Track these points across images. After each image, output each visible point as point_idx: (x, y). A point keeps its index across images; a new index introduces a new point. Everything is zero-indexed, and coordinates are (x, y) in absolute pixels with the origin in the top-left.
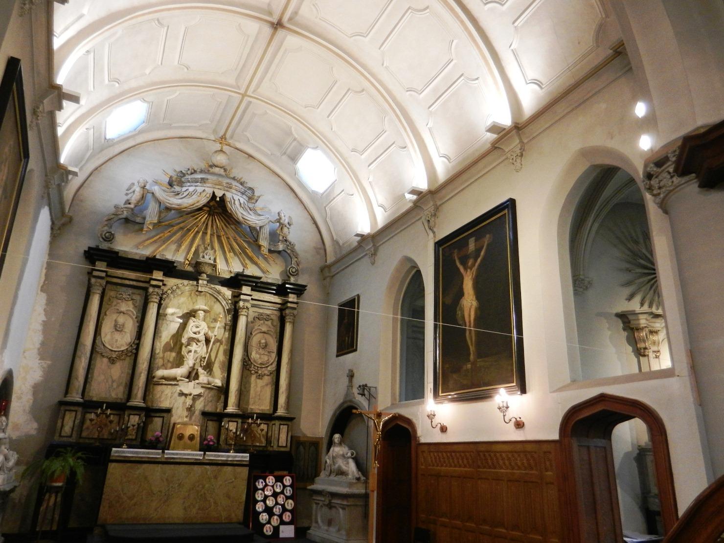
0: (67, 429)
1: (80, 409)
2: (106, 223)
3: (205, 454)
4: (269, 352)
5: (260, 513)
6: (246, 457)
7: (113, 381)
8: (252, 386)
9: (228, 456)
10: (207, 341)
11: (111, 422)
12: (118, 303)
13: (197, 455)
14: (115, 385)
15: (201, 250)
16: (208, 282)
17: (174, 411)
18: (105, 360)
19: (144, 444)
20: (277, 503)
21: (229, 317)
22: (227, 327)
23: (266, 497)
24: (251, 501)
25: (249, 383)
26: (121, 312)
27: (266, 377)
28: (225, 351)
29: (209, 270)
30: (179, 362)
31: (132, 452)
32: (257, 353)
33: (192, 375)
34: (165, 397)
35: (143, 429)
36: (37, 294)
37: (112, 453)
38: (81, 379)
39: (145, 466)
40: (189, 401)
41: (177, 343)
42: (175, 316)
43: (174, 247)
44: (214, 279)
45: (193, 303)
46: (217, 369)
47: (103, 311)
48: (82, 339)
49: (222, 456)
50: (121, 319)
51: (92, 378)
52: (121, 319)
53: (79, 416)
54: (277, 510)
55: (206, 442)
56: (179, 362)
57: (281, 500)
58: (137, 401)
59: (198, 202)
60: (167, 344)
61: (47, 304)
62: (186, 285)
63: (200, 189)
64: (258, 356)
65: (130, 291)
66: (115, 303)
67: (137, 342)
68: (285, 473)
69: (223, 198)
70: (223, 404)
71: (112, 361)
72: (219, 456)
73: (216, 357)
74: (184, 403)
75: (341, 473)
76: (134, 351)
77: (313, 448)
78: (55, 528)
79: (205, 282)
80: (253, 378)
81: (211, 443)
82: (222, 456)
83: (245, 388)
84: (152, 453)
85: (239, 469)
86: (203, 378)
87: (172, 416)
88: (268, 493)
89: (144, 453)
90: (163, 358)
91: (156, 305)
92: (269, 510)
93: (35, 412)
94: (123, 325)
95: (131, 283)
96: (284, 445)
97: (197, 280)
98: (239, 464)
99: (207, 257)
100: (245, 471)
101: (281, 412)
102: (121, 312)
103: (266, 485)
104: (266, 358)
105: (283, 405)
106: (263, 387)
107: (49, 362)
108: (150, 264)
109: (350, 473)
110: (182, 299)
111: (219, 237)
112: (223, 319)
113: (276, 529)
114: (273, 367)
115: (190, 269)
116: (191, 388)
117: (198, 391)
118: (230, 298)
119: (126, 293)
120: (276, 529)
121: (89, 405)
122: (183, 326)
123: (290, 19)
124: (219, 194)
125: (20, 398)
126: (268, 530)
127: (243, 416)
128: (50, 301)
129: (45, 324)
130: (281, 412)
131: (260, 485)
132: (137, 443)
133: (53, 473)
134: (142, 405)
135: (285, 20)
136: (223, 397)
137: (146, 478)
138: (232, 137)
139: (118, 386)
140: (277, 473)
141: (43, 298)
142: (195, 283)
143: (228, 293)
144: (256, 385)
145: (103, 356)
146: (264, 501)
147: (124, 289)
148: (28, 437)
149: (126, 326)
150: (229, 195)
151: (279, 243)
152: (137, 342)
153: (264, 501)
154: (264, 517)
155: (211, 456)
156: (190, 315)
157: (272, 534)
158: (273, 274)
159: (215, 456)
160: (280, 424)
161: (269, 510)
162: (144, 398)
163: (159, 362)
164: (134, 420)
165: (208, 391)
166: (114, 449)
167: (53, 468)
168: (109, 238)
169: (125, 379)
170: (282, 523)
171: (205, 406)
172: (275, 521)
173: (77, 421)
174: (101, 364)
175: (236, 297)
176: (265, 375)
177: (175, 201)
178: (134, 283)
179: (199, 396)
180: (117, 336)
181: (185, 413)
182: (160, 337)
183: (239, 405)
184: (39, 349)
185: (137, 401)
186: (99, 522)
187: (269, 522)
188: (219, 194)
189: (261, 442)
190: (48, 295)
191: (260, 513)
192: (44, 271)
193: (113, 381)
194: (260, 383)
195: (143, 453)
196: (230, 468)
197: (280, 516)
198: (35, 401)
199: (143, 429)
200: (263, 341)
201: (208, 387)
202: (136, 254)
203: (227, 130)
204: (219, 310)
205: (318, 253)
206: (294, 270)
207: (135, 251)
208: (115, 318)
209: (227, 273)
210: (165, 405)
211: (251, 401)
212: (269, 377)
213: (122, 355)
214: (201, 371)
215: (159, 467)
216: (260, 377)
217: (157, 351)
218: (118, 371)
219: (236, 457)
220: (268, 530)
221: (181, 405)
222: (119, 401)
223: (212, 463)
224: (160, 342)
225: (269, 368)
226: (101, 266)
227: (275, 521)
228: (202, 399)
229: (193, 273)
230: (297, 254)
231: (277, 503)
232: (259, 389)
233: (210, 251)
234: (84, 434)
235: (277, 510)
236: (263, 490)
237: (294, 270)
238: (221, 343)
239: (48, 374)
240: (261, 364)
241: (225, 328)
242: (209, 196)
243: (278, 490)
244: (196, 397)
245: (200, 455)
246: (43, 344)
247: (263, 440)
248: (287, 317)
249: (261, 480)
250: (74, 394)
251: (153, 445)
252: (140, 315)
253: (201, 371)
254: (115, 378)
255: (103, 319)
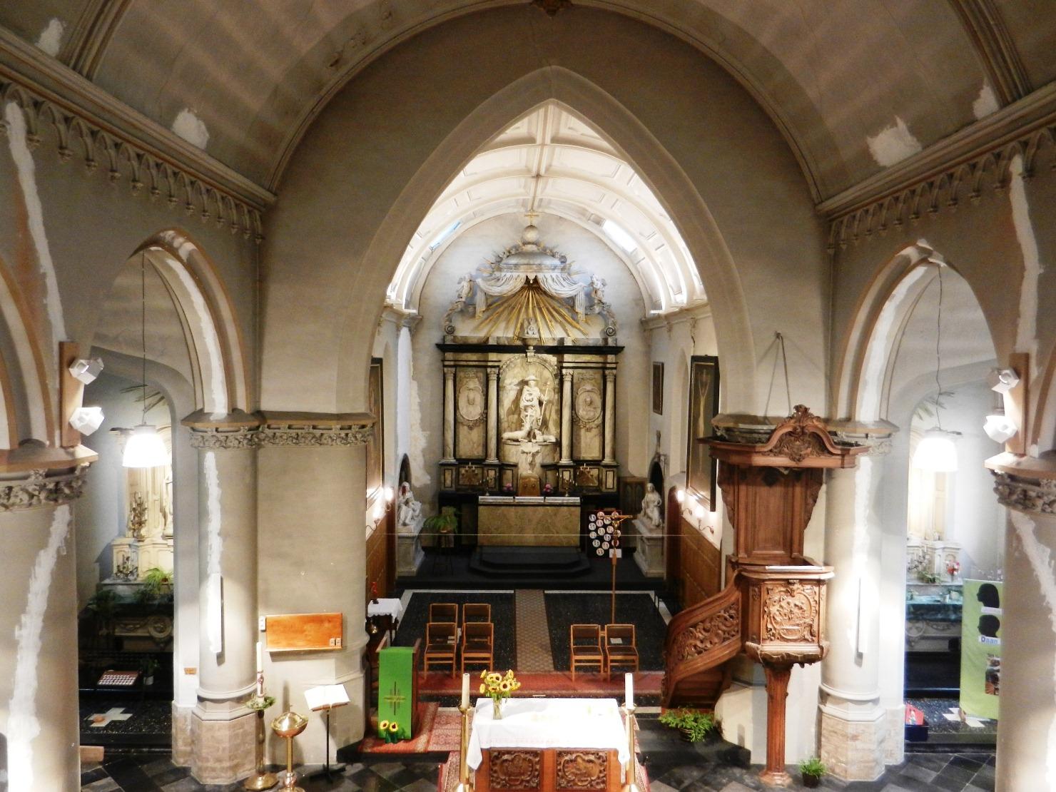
0: (448, 482)
1: (454, 468)
2: (446, 318)
3: (545, 498)
4: (595, 408)
5: (593, 540)
6: (577, 500)
7: (474, 443)
8: (582, 438)
9: (563, 500)
10: (541, 403)
11: (477, 474)
12: (467, 382)
13: (539, 499)
14: (475, 445)
15: (525, 326)
16: (535, 353)
17: (519, 466)
18: (466, 428)
19: (502, 493)
20: (606, 533)
21: (557, 381)
22: (556, 390)
23: (597, 528)
24: (585, 529)
25: (579, 435)
26: (470, 390)
27: (593, 429)
28: (557, 411)
29: (535, 343)
30: (520, 425)
31: (492, 499)
32: (584, 410)
33: (531, 436)
34: (512, 454)
35: (499, 479)
36: (410, 383)
37: (479, 500)
38: (451, 446)
39: (503, 508)
40: (530, 459)
41: (516, 407)
42: (512, 385)
43: (503, 325)
44: (541, 349)
45: (526, 371)
46: (551, 426)
47: (457, 389)
48: (446, 416)
49: (559, 500)
50: (472, 395)
51: (459, 441)
52: (472, 395)
53: (454, 473)
54: (607, 538)
55: (544, 490)
56: (520, 425)
57: (610, 529)
58: (492, 460)
59: (515, 288)
60: (510, 409)
61: (418, 390)
62: (517, 358)
63: (515, 275)
64: (585, 413)
65: (475, 370)
66: (465, 382)
67: (485, 411)
68: (613, 509)
69: (536, 280)
70: (559, 455)
71: (471, 428)
72: (556, 500)
73: (550, 415)
74: (526, 459)
75: (650, 518)
76: (485, 419)
77: (639, 487)
78: (452, 546)
79: (533, 354)
80: (583, 432)
81: (549, 491)
82: (559, 500)
83: (576, 440)
84: (506, 499)
85: (573, 509)
86: (540, 438)
87: (518, 469)
88: (600, 523)
89: (501, 499)
90: (508, 421)
91: (495, 382)
92: (601, 539)
93: (427, 467)
94: (474, 400)
95: (474, 363)
96: (611, 487)
97: (526, 353)
98: (574, 505)
99: (530, 333)
100: (578, 510)
101: (607, 460)
102: (470, 390)
103: (597, 519)
104: (592, 414)
105: (609, 455)
106: (592, 439)
107: (428, 432)
108: (483, 347)
109: (654, 519)
110: (516, 370)
111: (540, 309)
112: (552, 383)
113: (607, 552)
114: (600, 420)
115: (519, 343)
116: (531, 447)
117: (537, 448)
118: (556, 363)
119: (471, 372)
120: (607, 552)
121: (462, 462)
122: (520, 392)
123: (547, 170)
124: (532, 277)
125: (415, 460)
126: (600, 552)
127: (577, 463)
128: (420, 386)
129: (421, 405)
130: (607, 460)
131: (592, 518)
132: (496, 490)
133: (440, 527)
134: (496, 462)
135: (542, 172)
136: (558, 449)
137: (505, 516)
138: (539, 206)
139: (478, 446)
140: (605, 510)
141: (415, 384)
142: (524, 355)
143: (552, 359)
144: (586, 437)
145: (464, 425)
146: (596, 531)
147: (470, 369)
148: (426, 486)
149: (476, 400)
150: (540, 276)
151: (595, 307)
152: (485, 411)
153: (596, 531)
154: (596, 543)
155: (550, 500)
156: (524, 383)
157: (489, 603)
158: (593, 335)
159: (553, 500)
160: (606, 471)
161: (601, 539)
162: (498, 456)
163: (504, 425)
164: (492, 473)
165: (544, 447)
166: (480, 497)
167: (439, 524)
168: (451, 331)
169: (482, 441)
170: (611, 547)
171: (543, 459)
172: (606, 546)
173: (454, 476)
174: (463, 431)
175: (561, 362)
176: (592, 428)
177: (496, 290)
178: (477, 363)
179: (538, 452)
180: (471, 408)
181: (528, 467)
182: (503, 405)
183: (571, 456)
184: (420, 424)
185: (492, 460)
186: (479, 544)
187: (601, 547)
188: (532, 277)
189: (593, 482)
190: (418, 382)
191: (593, 540)
192: (412, 364)
193: (474, 443)
194: (590, 435)
195: (500, 499)
196: (565, 508)
197: (610, 542)
198: (425, 461)
199: (499, 479)
200: (588, 399)
201: (545, 444)
202: (475, 337)
203: (533, 204)
204: (548, 375)
205: (637, 305)
206: (611, 331)
207: (472, 335)
208: (466, 394)
209: (551, 341)
210: (512, 460)
211: (583, 451)
212: (597, 430)
213: (476, 423)
214: (537, 432)
215: (513, 509)
216: (589, 430)
217: (502, 417)
218: (476, 435)
219: (569, 500)
220: (600, 552)
221: (524, 460)
222: (480, 457)
223: (551, 505)
224: (503, 409)
225: (596, 422)
226: (449, 356)
227: (606, 546)
228: (540, 454)
229: (521, 348)
230: (614, 314)
231: (606, 533)
232: (588, 440)
233: (533, 326)
234: (461, 482)
235: (607, 538)
236: (595, 522)
237: (611, 331)
238: (553, 404)
239: (429, 442)
240: (588, 419)
241: (554, 391)
242: (523, 281)
243: (607, 522)
244: (534, 455)
245: (542, 499)
246: (422, 420)
247: (596, 482)
248: (608, 377)
249: (593, 515)
250: (448, 457)
251: (509, 493)
252: (485, 389)
253: (537, 432)
254: (474, 441)
255: (458, 396)
